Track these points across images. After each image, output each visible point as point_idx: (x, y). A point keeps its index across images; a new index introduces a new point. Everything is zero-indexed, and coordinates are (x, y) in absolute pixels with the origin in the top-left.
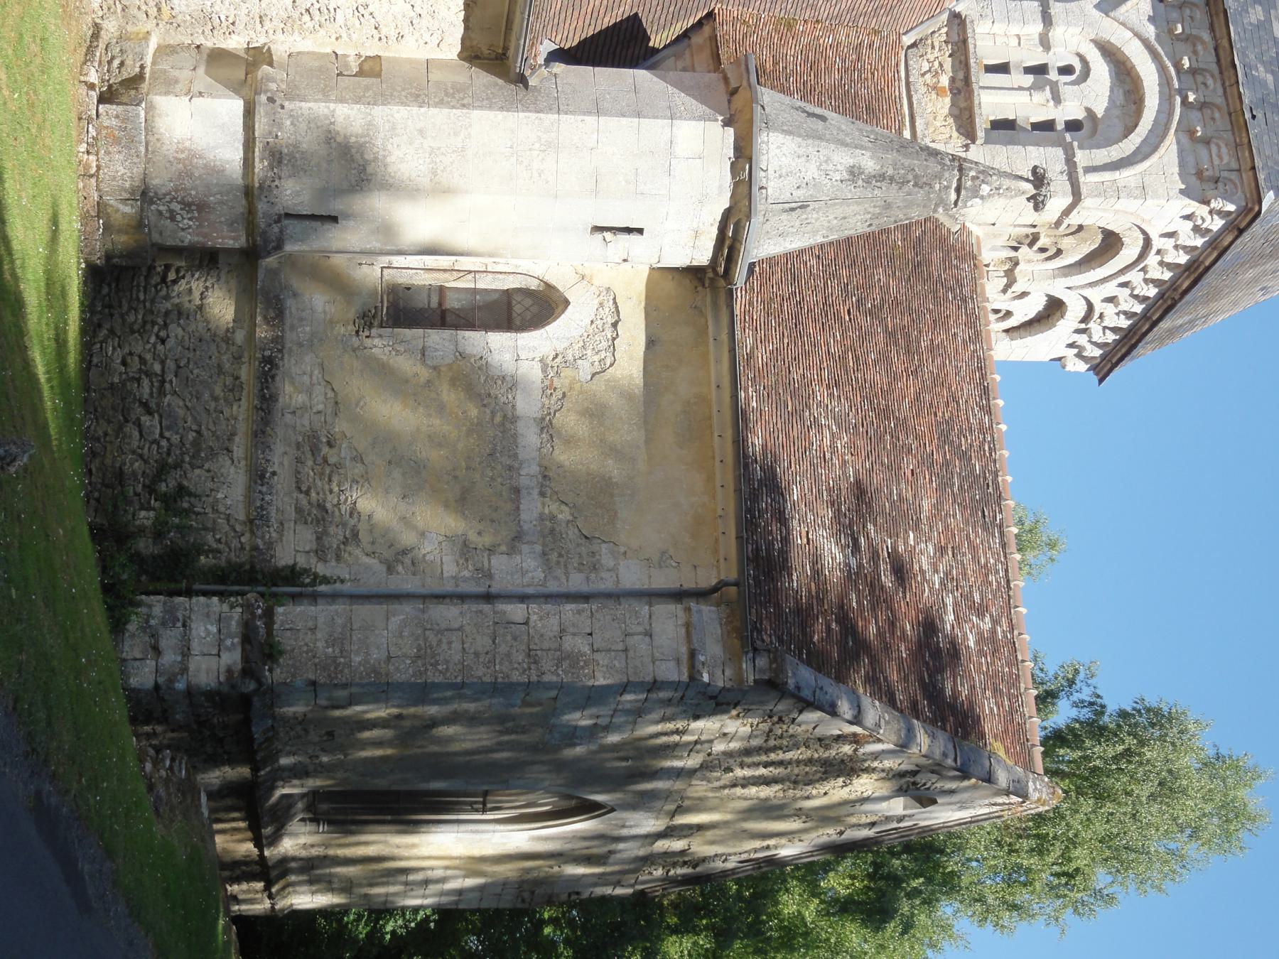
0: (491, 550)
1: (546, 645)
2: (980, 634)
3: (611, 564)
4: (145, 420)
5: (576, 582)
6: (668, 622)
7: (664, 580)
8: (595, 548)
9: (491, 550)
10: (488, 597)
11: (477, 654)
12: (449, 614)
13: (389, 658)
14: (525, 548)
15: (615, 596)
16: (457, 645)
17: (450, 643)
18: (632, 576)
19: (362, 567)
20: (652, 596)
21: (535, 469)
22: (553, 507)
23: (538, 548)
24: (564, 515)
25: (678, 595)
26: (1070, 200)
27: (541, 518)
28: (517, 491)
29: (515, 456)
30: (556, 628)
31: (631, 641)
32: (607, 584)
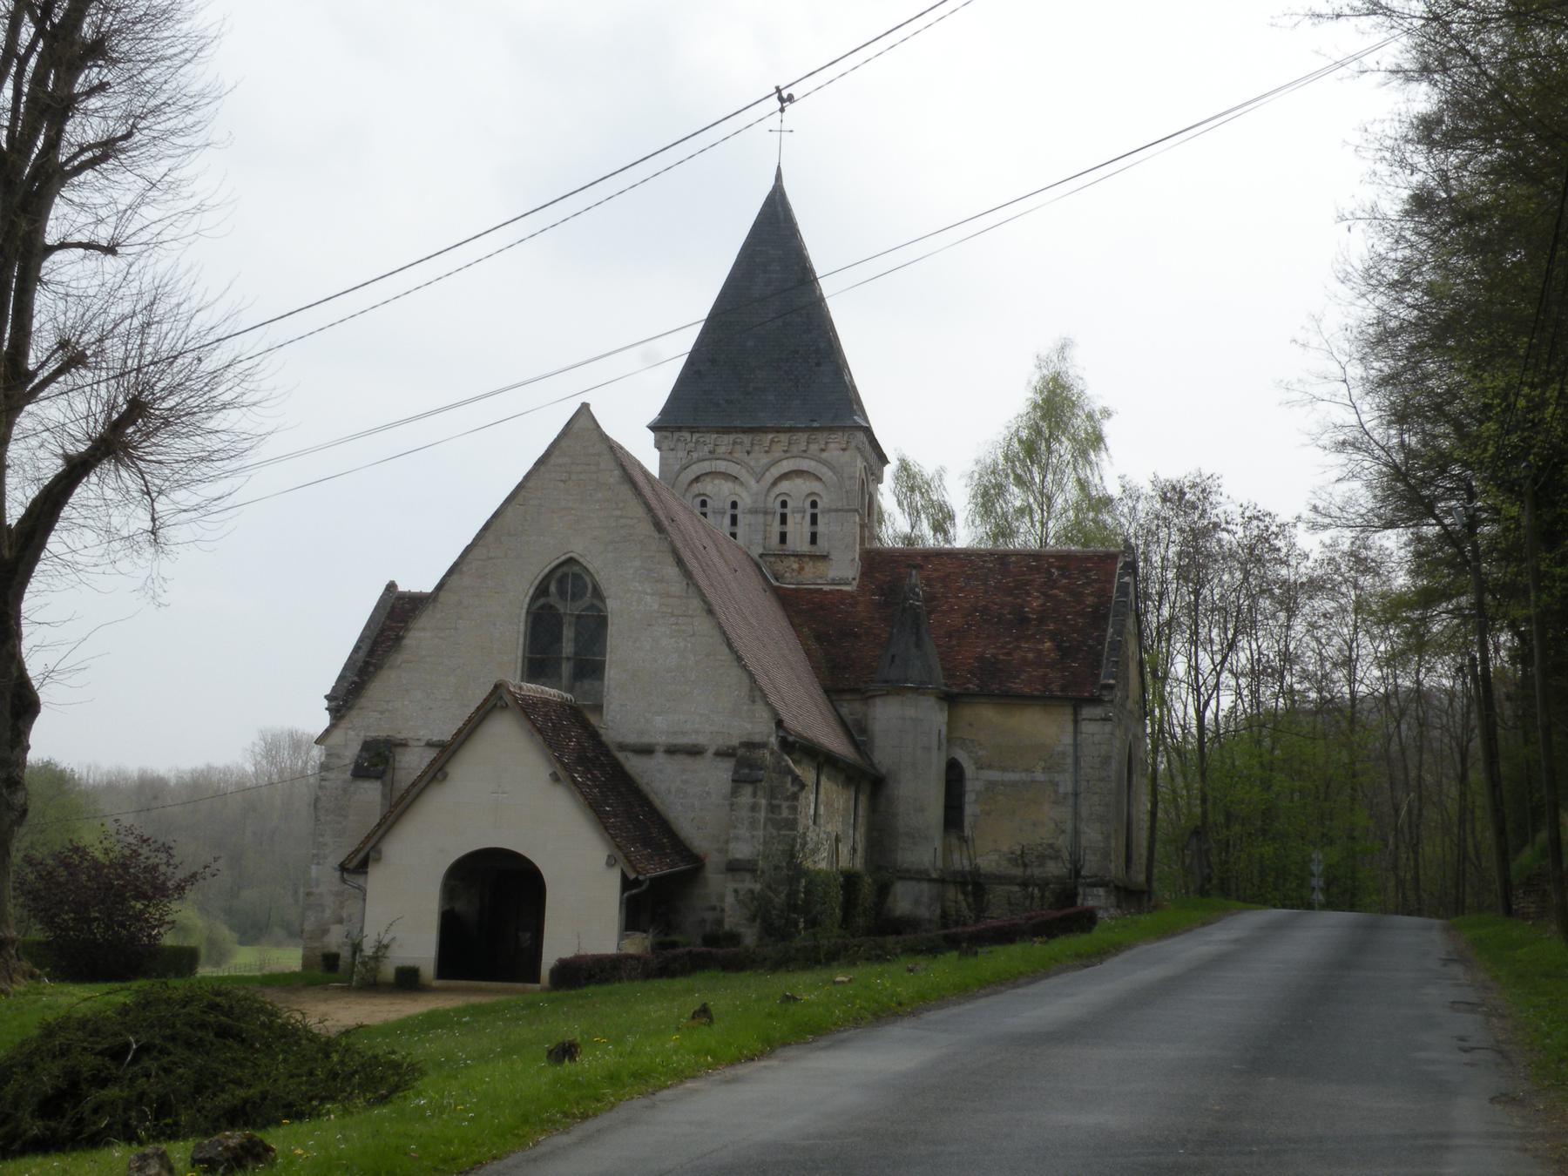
0: (1056, 792)
2: (1063, 576)
5: (1070, 760)
6: (1088, 728)
7: (1070, 728)
10: (1076, 795)
15: (1076, 745)
18: (1068, 739)
19: (1063, 842)
20: (1076, 732)
25: (1076, 722)
32: (1070, 750)
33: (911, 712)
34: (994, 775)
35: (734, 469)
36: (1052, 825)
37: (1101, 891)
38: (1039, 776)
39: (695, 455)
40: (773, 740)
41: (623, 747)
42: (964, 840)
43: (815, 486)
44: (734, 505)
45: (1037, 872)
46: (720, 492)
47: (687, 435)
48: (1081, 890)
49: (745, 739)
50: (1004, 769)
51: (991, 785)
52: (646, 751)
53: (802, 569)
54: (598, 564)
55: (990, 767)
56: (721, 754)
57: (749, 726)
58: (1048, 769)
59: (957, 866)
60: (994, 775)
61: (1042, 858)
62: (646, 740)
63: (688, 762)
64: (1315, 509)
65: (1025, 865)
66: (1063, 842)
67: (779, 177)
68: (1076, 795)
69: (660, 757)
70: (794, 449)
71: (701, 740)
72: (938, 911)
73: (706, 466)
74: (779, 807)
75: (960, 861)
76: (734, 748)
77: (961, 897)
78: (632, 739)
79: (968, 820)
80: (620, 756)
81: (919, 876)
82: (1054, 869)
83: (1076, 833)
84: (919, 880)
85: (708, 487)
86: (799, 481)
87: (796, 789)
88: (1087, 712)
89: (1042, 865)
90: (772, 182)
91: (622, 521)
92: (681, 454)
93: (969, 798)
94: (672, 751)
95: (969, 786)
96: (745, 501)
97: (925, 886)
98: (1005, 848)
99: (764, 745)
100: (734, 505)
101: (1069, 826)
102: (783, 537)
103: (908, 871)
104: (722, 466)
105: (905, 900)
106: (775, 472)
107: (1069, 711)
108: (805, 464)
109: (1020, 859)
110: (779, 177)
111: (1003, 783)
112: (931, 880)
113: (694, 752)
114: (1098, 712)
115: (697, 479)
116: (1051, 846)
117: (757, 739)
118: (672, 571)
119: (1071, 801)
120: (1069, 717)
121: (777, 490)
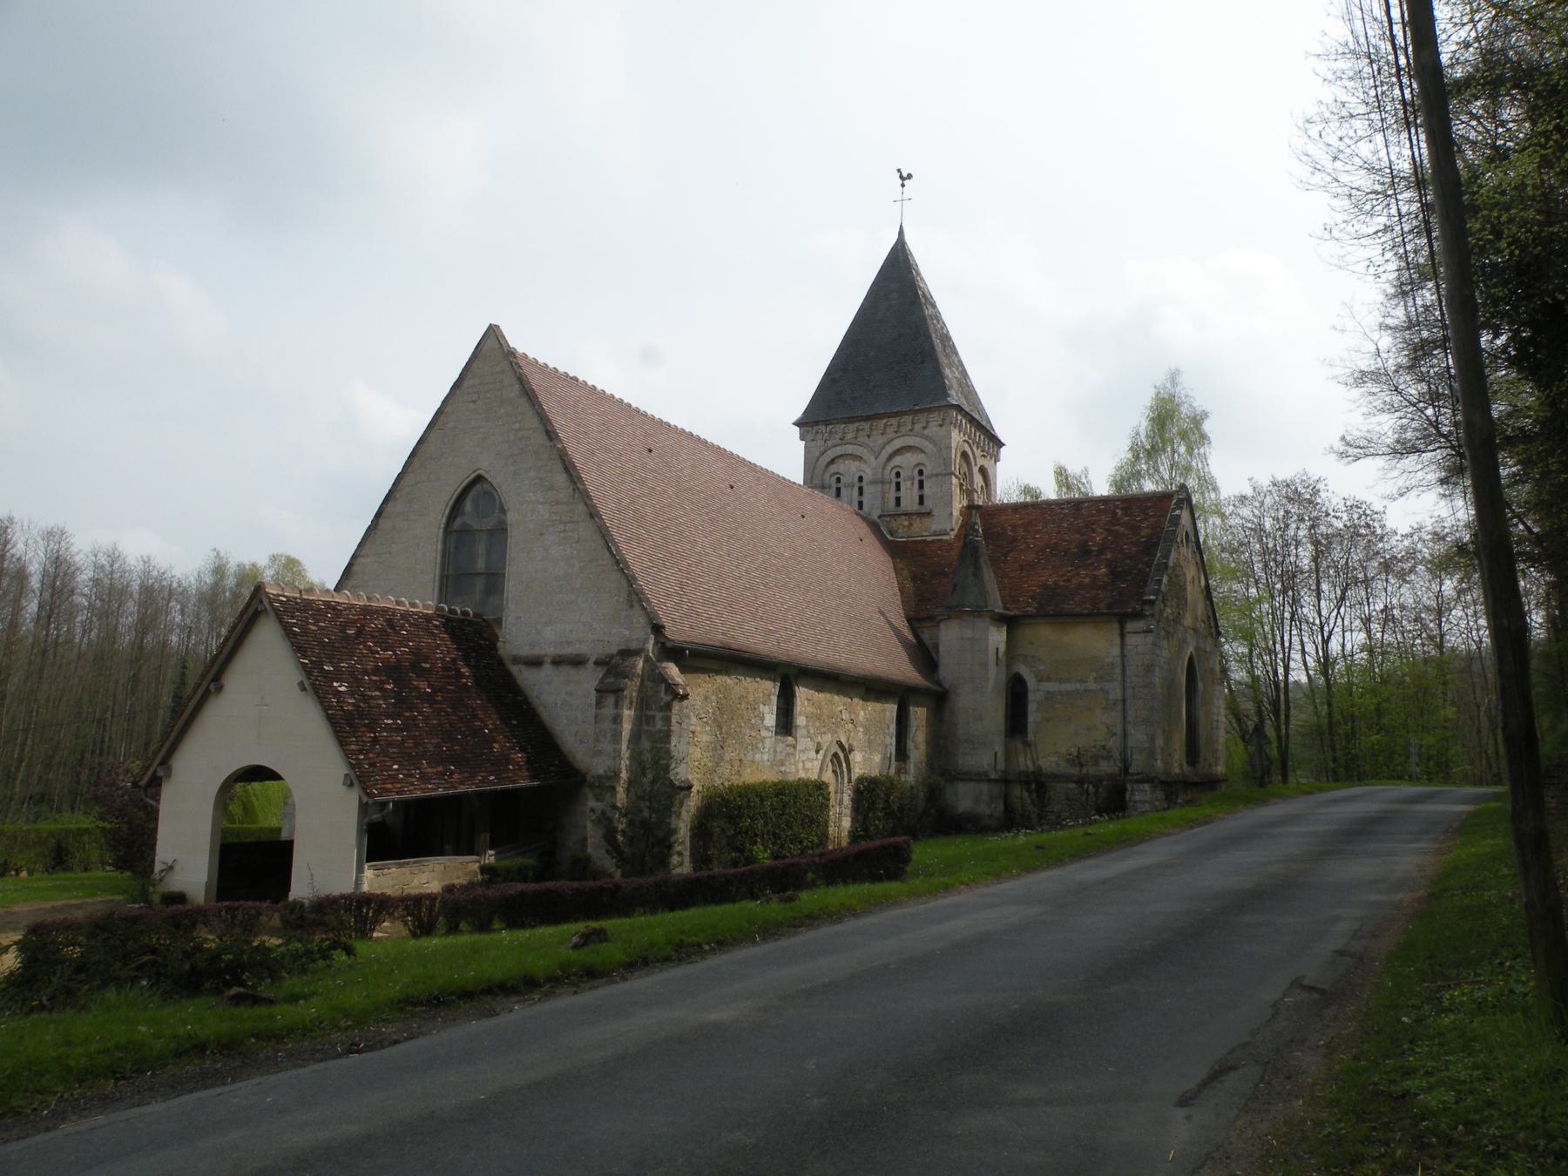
5: (1118, 670)
6: (1132, 640)
7: (1117, 641)
10: (1124, 701)
12: (1131, 715)
15: (1123, 656)
18: (1116, 651)
19: (1114, 743)
25: (1122, 636)
32: (1119, 660)
33: (968, 633)
34: (1052, 686)
35: (858, 450)
37: (1147, 787)
38: (1092, 685)
40: (650, 646)
41: (517, 660)
42: (1027, 744)
43: (921, 458)
44: (861, 479)
45: (1092, 770)
46: (849, 469)
47: (822, 428)
48: (1129, 786)
49: (623, 647)
50: (1060, 681)
51: (1050, 696)
52: (535, 663)
54: (498, 478)
55: (1049, 679)
56: (597, 663)
57: (627, 633)
58: (1098, 679)
59: (1022, 768)
60: (1052, 686)
61: (1096, 759)
62: (536, 652)
63: (572, 672)
64: (1348, 444)
65: (1081, 765)
66: (1114, 743)
67: (901, 232)
68: (1124, 701)
69: (548, 669)
70: (903, 430)
71: (584, 649)
72: (1001, 807)
73: (838, 451)
74: (654, 717)
75: (1024, 763)
76: (612, 657)
77: (1026, 794)
78: (525, 651)
79: (1031, 727)
80: (514, 669)
81: (981, 777)
82: (1106, 768)
83: (1125, 734)
84: (979, 781)
85: (840, 467)
86: (908, 455)
87: (669, 698)
88: (1130, 626)
89: (1096, 764)
90: (896, 237)
91: (520, 434)
92: (820, 443)
93: (1032, 707)
94: (558, 662)
95: (1031, 697)
96: (868, 474)
97: (985, 787)
98: (1063, 751)
99: (637, 652)
100: (861, 479)
101: (1118, 730)
102: (898, 500)
103: (967, 773)
104: (849, 449)
105: (964, 798)
106: (889, 449)
107: (1116, 625)
108: (911, 441)
109: (1077, 760)
110: (901, 232)
111: (1061, 693)
112: (990, 781)
113: (577, 662)
114: (1141, 625)
115: (832, 461)
116: (1103, 747)
117: (634, 646)
118: (561, 478)
119: (1120, 707)
120: (1116, 632)
121: (892, 464)
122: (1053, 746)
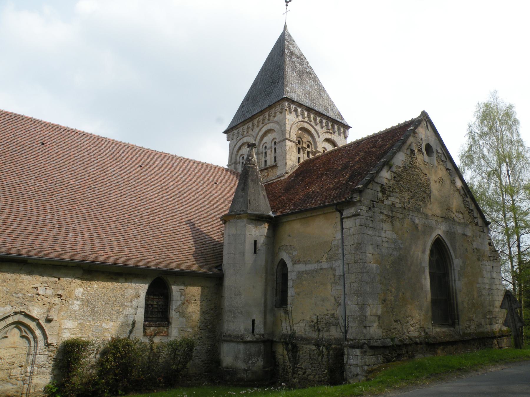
0: (334, 275)
1: (353, 258)
3: (337, 241)
4: (307, 373)
8: (333, 246)
9: (334, 275)
11: (356, 278)
13: (358, 304)
14: (334, 266)
16: (354, 284)
17: (354, 286)
18: (339, 236)
21: (316, 265)
22: (324, 258)
23: (334, 262)
24: (326, 256)
26: (287, 141)
27: (327, 262)
28: (321, 269)
29: (314, 270)
30: (349, 255)
31: (352, 234)
33: (233, 231)
34: (301, 267)
36: (333, 300)
37: (358, 352)
38: (325, 265)
39: (238, 139)
42: (286, 312)
45: (325, 335)
48: (346, 350)
50: (306, 263)
51: (300, 273)
53: (268, 175)
55: (299, 262)
58: (330, 259)
59: (285, 331)
60: (301, 267)
61: (328, 325)
65: (319, 330)
66: (339, 312)
67: (285, 27)
70: (266, 121)
72: (260, 363)
75: (285, 328)
77: (285, 352)
79: (289, 299)
81: (239, 339)
82: (335, 333)
84: (237, 342)
86: (269, 135)
88: (348, 212)
89: (328, 330)
90: (283, 30)
93: (290, 284)
97: (241, 347)
98: (308, 318)
103: (230, 336)
105: (230, 356)
106: (260, 134)
107: (338, 214)
109: (316, 326)
110: (285, 27)
111: (306, 272)
116: (333, 315)
121: (263, 143)
122: (303, 315)
